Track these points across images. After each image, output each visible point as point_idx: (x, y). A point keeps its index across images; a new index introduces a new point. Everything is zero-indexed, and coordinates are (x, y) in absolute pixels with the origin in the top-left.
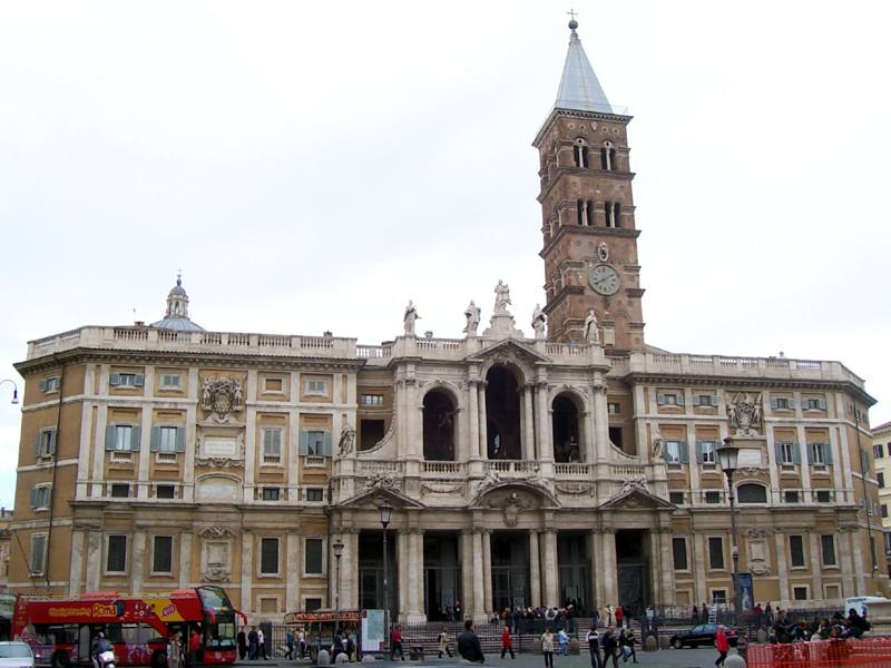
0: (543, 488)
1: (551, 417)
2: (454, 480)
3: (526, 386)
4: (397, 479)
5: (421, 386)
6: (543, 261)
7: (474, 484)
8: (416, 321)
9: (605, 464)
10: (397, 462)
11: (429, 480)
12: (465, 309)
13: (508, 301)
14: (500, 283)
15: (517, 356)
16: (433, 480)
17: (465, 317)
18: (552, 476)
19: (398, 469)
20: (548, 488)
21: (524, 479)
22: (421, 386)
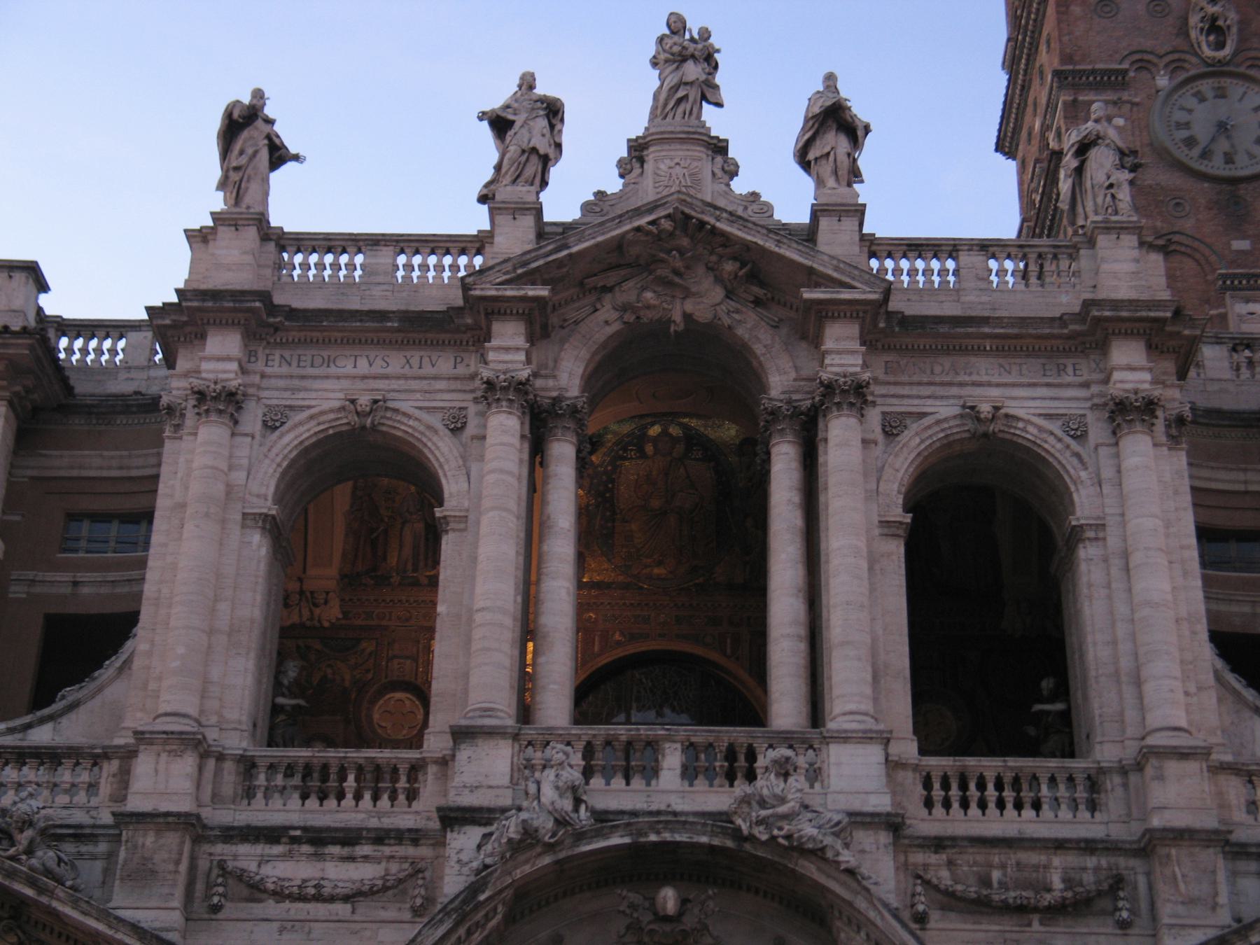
0: (818, 853)
1: (896, 550)
2: (380, 837)
3: (774, 413)
4: (80, 835)
5: (270, 426)
6: (1011, 166)
7: (465, 841)
8: (276, 177)
9: (1183, 754)
10: (97, 758)
11: (271, 835)
12: (495, 101)
13: (708, 93)
14: (677, 25)
15: (729, 295)
16: (271, 835)
17: (485, 124)
18: (881, 803)
19: (105, 788)
20: (847, 858)
21: (721, 819)
22: (270, 426)
